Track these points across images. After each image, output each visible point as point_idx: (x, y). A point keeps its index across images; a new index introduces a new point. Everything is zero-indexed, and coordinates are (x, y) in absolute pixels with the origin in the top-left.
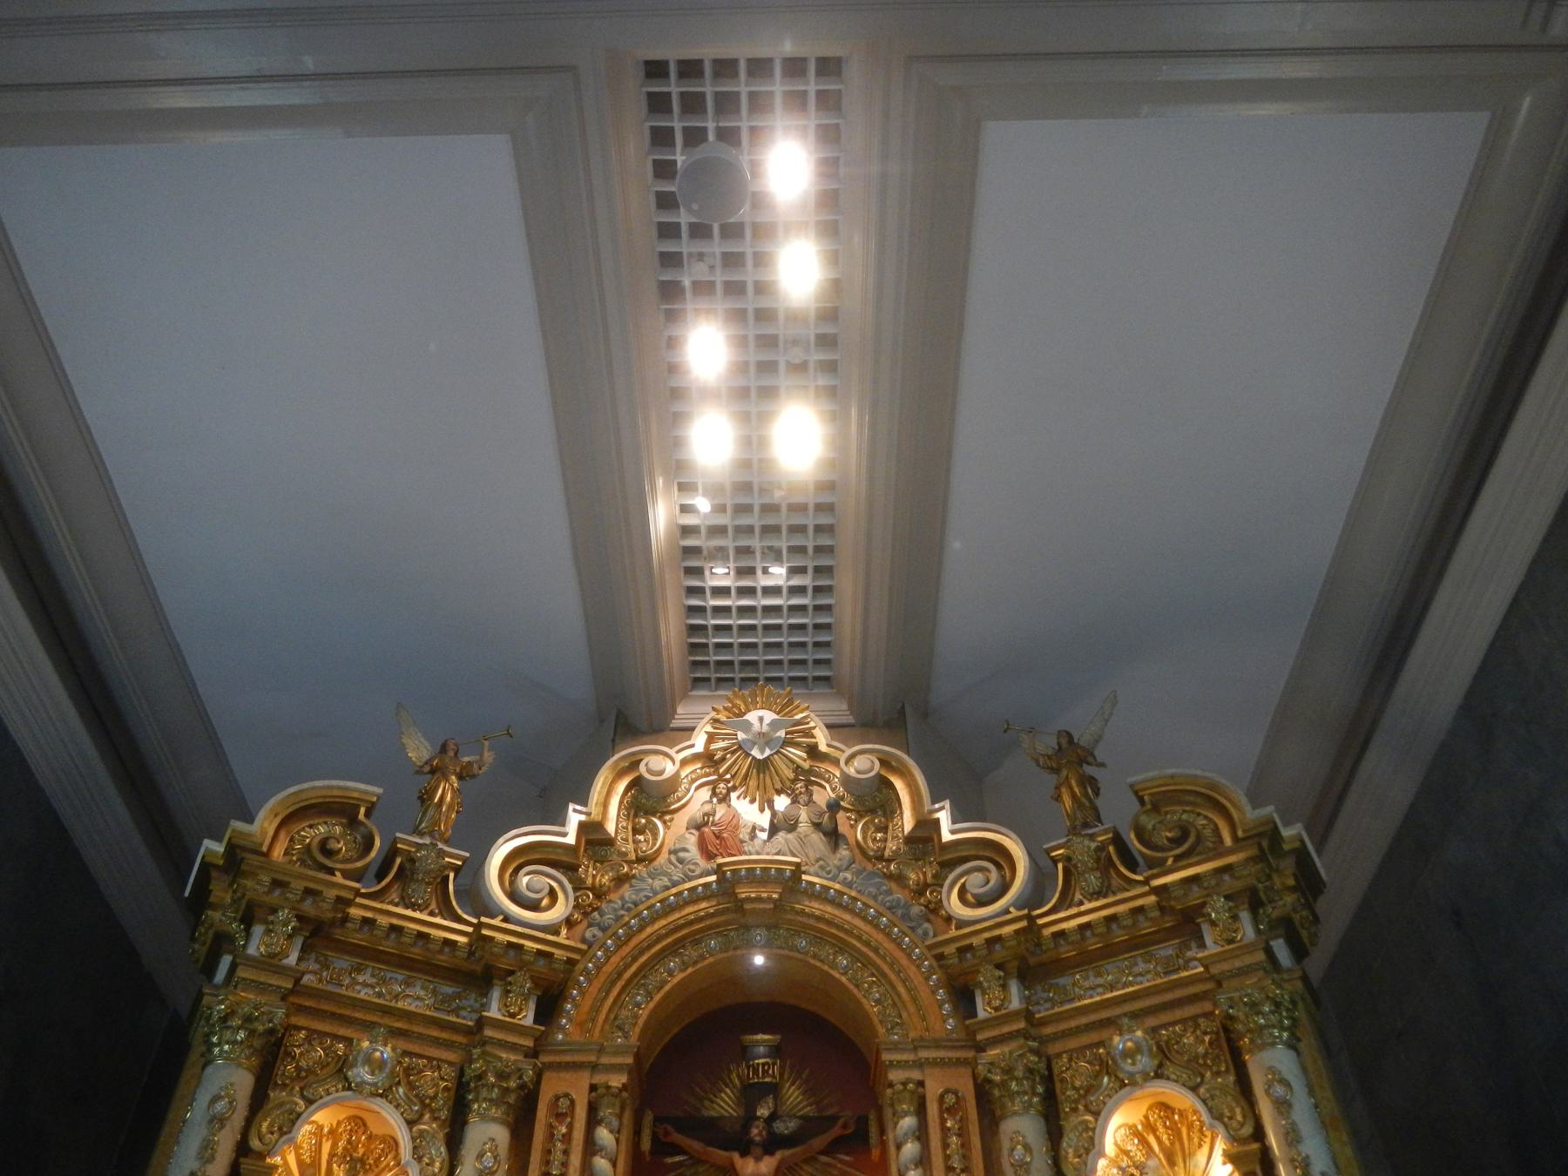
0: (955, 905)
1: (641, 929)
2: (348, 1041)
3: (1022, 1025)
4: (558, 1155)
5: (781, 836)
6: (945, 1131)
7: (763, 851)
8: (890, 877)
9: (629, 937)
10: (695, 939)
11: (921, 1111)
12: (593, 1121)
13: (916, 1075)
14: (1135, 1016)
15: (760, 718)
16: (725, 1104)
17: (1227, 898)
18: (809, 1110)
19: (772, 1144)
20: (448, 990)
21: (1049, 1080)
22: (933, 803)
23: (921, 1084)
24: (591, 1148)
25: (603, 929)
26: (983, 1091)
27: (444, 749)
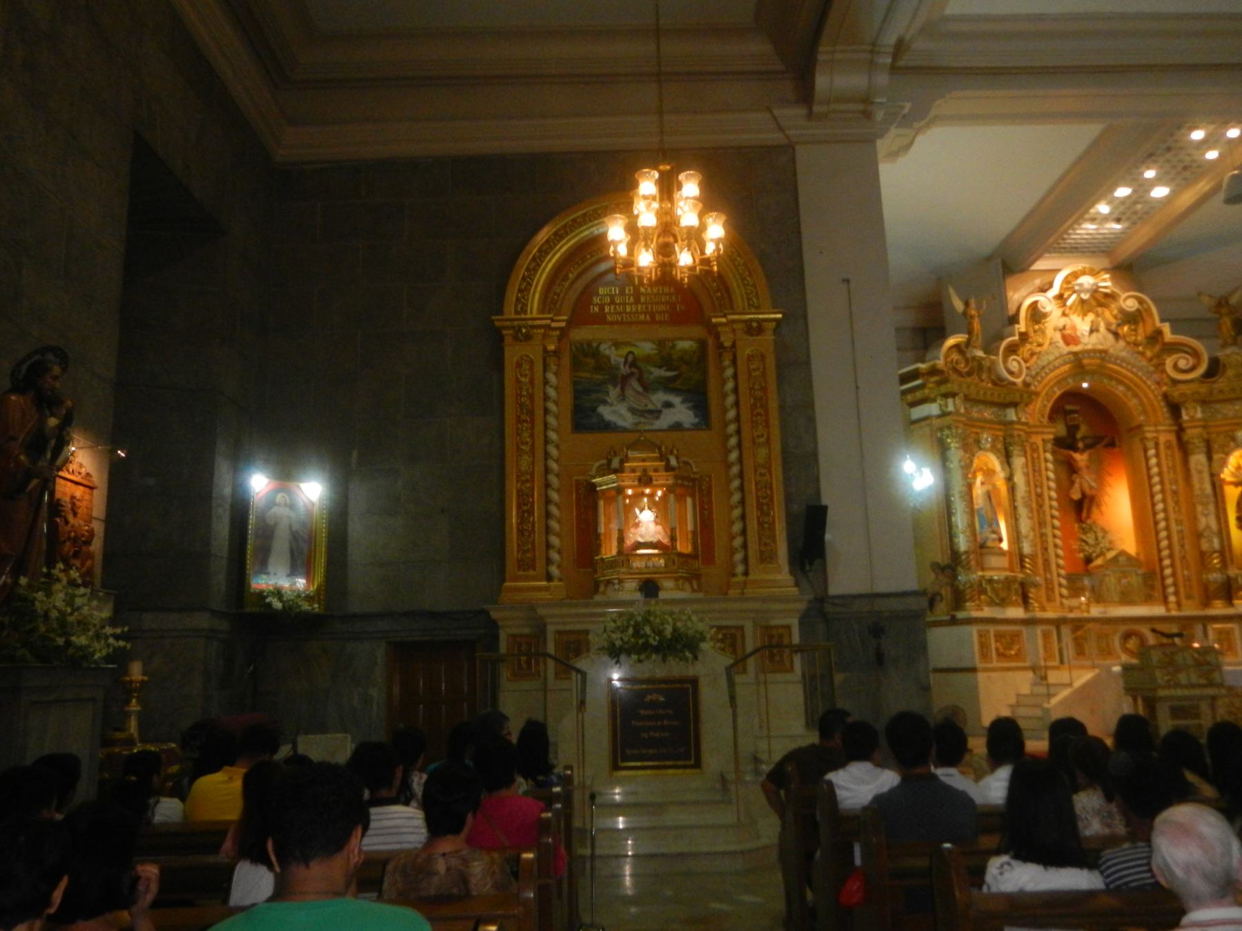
0: (1169, 366)
1: (1047, 374)
2: (977, 433)
3: (1201, 423)
4: (1037, 465)
5: (1095, 335)
6: (1167, 455)
7: (1089, 342)
8: (1139, 353)
9: (1042, 378)
10: (1065, 379)
11: (1157, 446)
12: (1045, 451)
13: (1155, 435)
15: (1087, 281)
19: (1087, 447)
20: (995, 409)
22: (1163, 320)
23: (1157, 438)
25: (1034, 377)
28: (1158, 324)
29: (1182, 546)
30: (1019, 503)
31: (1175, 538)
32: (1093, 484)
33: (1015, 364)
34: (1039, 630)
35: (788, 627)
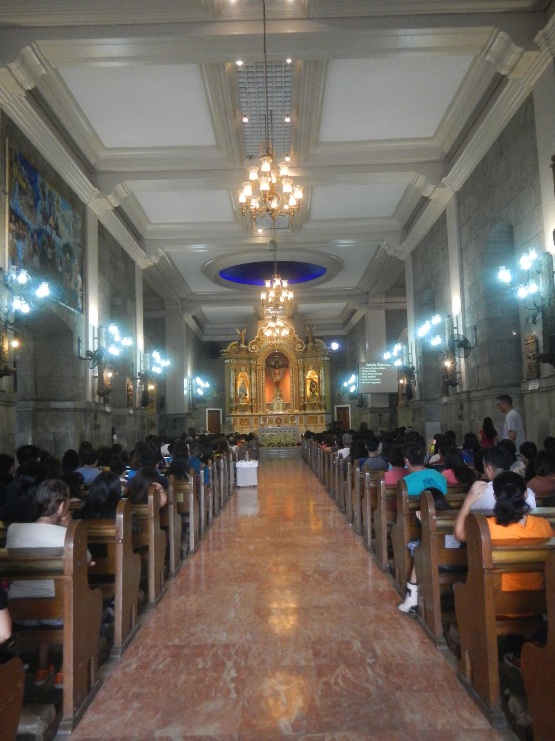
8: (290, 343)
11: (292, 369)
12: (262, 370)
14: (312, 364)
16: (273, 363)
17: (321, 356)
18: (282, 364)
21: (304, 368)
24: (262, 373)
26: (298, 369)
27: (241, 332)
28: (295, 336)
29: (296, 396)
30: (252, 385)
31: (294, 393)
32: (279, 378)
33: (254, 348)
34: (253, 418)
35: (155, 421)
